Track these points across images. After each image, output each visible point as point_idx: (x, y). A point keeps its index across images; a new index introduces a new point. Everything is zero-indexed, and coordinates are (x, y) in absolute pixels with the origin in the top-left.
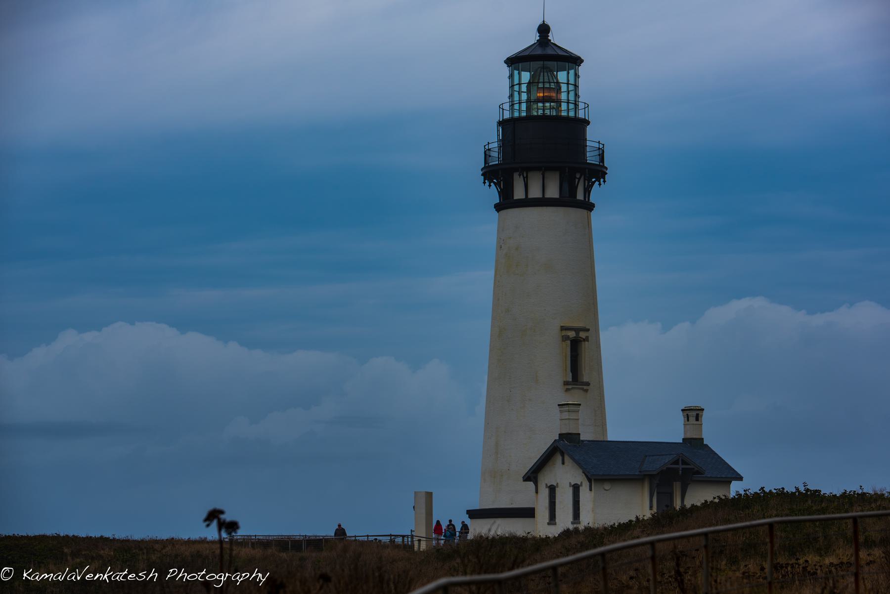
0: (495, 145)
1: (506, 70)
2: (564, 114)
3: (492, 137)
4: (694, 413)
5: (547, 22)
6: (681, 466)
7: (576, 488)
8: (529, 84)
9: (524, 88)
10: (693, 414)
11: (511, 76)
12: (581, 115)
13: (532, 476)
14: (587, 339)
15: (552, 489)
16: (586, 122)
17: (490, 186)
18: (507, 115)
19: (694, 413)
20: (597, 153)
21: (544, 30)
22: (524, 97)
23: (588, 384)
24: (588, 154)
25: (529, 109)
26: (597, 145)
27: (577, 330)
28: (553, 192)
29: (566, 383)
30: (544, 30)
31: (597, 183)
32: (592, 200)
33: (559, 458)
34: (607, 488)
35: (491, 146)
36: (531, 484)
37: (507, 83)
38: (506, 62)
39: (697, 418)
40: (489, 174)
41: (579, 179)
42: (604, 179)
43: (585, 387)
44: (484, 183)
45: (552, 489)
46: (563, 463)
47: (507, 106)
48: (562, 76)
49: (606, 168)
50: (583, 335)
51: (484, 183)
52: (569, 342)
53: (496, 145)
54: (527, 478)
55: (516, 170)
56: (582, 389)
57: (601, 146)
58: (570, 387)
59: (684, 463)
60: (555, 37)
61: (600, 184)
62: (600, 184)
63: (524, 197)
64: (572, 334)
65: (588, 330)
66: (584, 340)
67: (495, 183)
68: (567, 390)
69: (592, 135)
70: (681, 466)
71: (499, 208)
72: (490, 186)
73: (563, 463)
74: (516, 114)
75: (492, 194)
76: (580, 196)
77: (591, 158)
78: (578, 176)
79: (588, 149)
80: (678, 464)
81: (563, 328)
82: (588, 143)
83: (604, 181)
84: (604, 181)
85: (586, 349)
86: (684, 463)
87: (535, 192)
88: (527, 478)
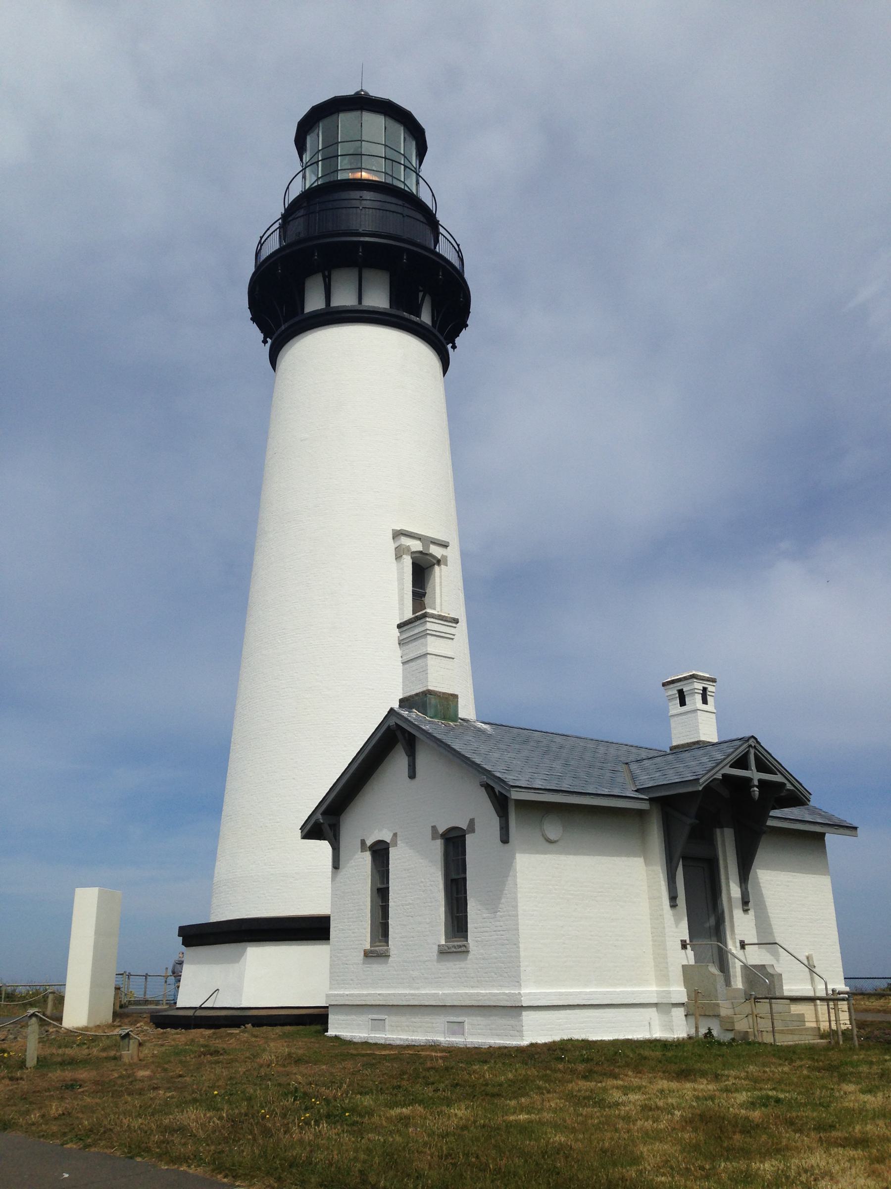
4: (699, 686)
6: (756, 776)
13: (325, 823)
15: (380, 853)
19: (699, 686)
33: (398, 762)
34: (552, 837)
36: (323, 847)
46: (412, 775)
50: (436, 551)
63: (323, 306)
65: (445, 545)
73: (412, 775)
81: (398, 534)
86: (762, 766)
88: (313, 830)
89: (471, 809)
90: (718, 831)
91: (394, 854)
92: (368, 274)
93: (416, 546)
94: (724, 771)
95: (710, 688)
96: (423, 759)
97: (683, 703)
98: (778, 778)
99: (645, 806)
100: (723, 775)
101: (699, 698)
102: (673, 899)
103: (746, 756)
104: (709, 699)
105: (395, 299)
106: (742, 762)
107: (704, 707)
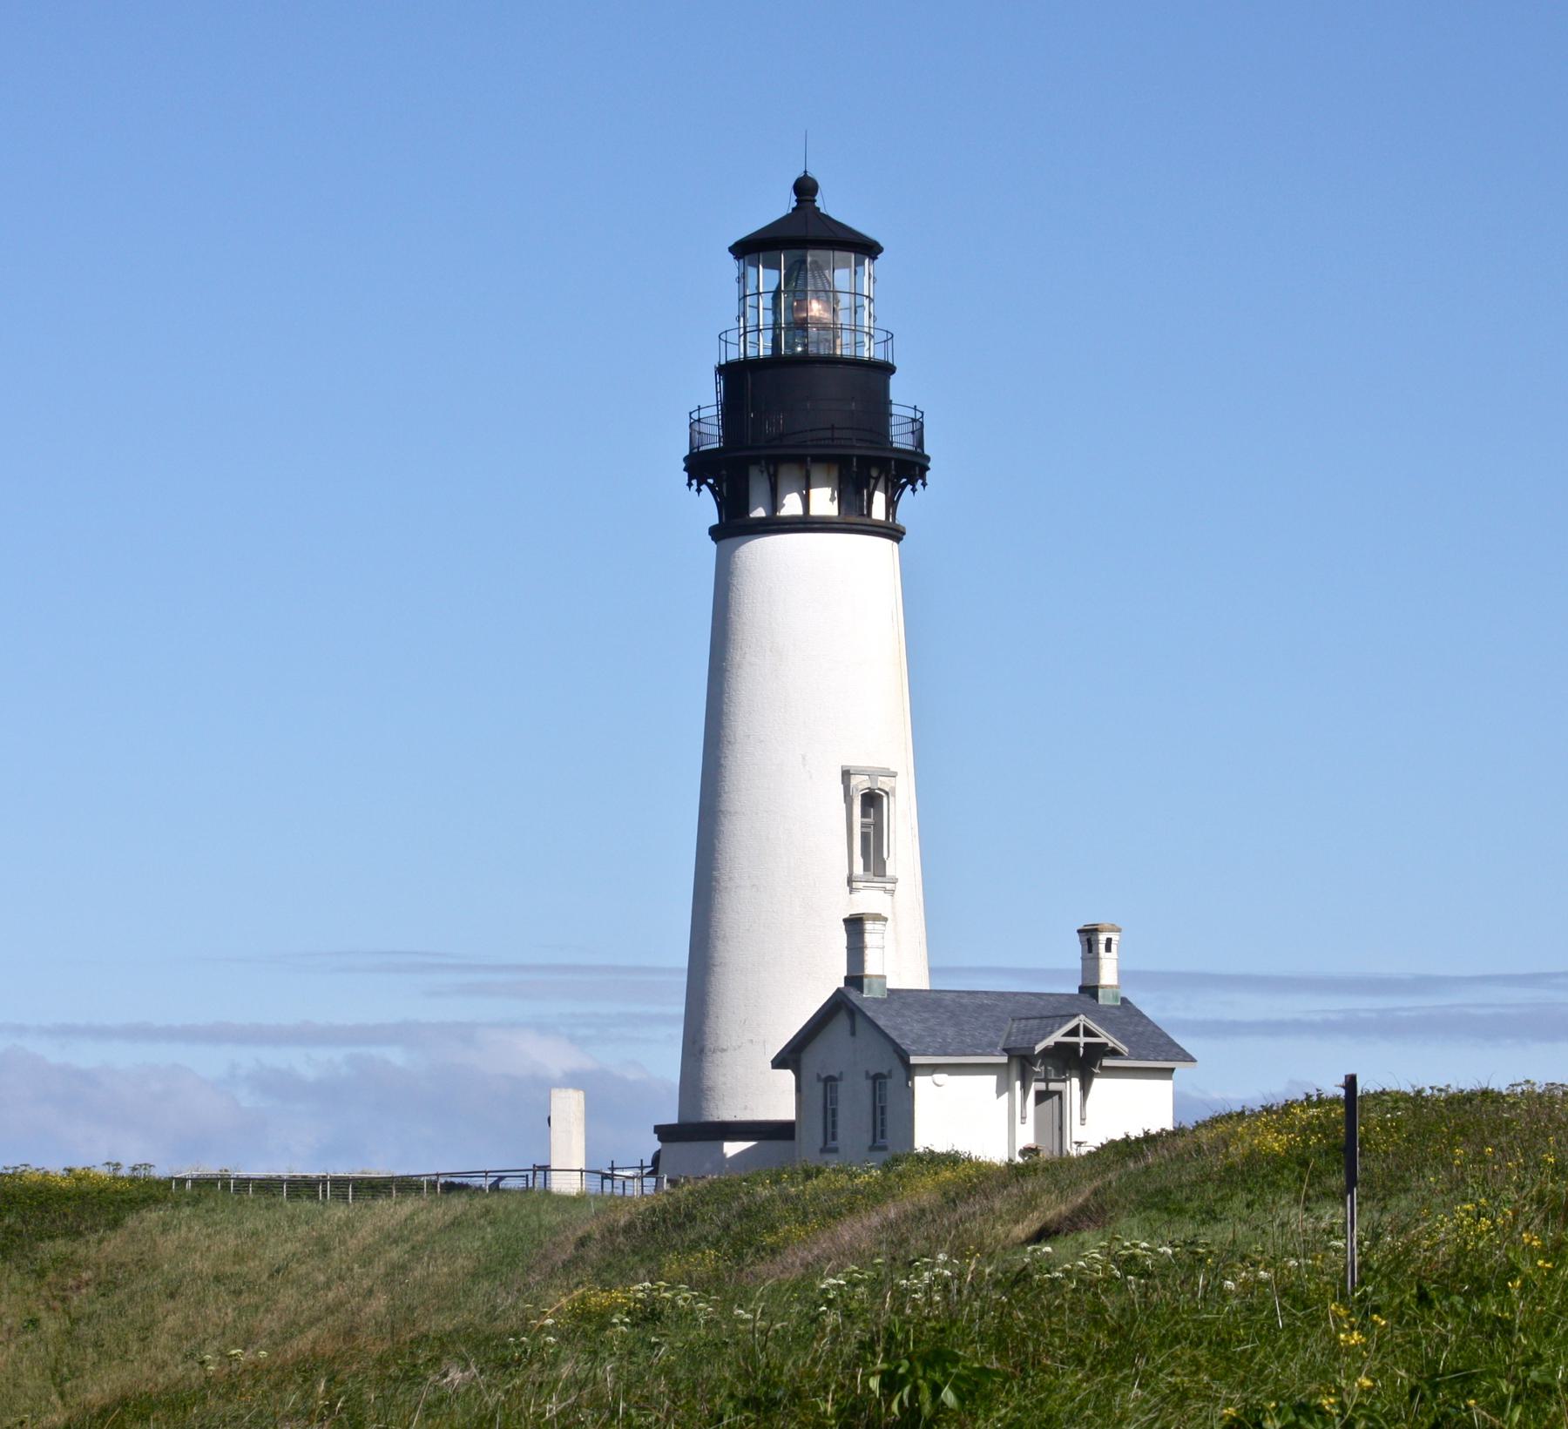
0: (712, 412)
1: (731, 265)
2: (847, 352)
3: (707, 395)
5: (812, 173)
7: (878, 1079)
8: (776, 295)
9: (765, 301)
11: (742, 279)
12: (880, 356)
16: (885, 369)
17: (699, 490)
18: (734, 354)
20: (910, 427)
21: (805, 189)
22: (766, 318)
24: (894, 430)
25: (776, 341)
26: (911, 414)
27: (872, 774)
28: (824, 502)
30: (805, 189)
31: (909, 487)
32: (902, 518)
35: (704, 413)
36: (788, 1076)
37: (734, 291)
38: (731, 250)
40: (699, 466)
41: (877, 480)
42: (923, 476)
43: (889, 886)
44: (690, 485)
45: (830, 1082)
46: (853, 1033)
47: (733, 337)
48: (842, 278)
49: (928, 459)
50: (883, 783)
51: (690, 485)
53: (713, 411)
54: (779, 1062)
55: (756, 461)
57: (919, 415)
58: (860, 885)
59: (1088, 1033)
60: (829, 203)
61: (914, 490)
62: (914, 490)
64: (860, 783)
65: (894, 775)
67: (709, 485)
69: (901, 392)
70: (1082, 1040)
71: (717, 533)
72: (699, 490)
73: (853, 1033)
74: (751, 353)
75: (705, 508)
76: (879, 510)
77: (901, 438)
78: (874, 473)
79: (894, 420)
82: (894, 409)
83: (924, 485)
84: (924, 485)
86: (1088, 1033)
87: (791, 505)
88: (779, 1062)
89: (889, 1063)
91: (842, 1087)
92: (817, 472)
95: (1115, 937)
96: (859, 1019)
97: (1090, 950)
99: (1004, 1060)
101: (1102, 947)
102: (1023, 1118)
104: (1114, 947)
106: (1074, 1032)
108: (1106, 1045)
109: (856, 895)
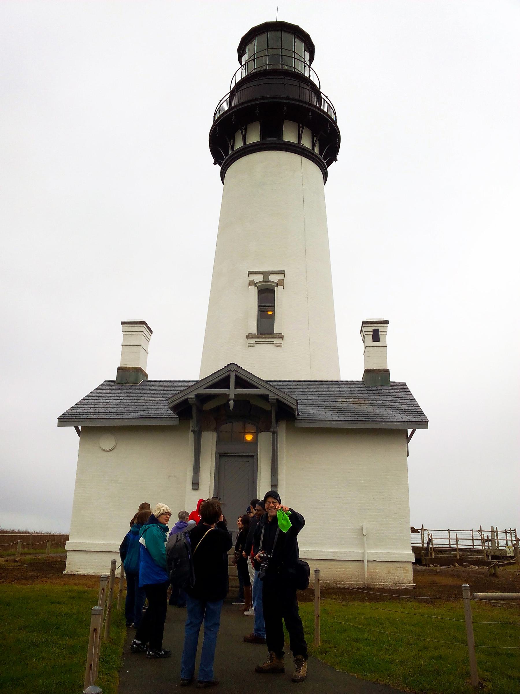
4: (370, 329)
10: (375, 331)
14: (281, 283)
23: (281, 337)
29: (249, 337)
39: (376, 336)
43: (276, 341)
50: (274, 278)
52: (254, 291)
56: (272, 343)
65: (283, 273)
66: (277, 285)
68: (250, 345)
70: (232, 392)
80: (228, 387)
85: (282, 298)
90: (259, 434)
93: (259, 278)
94: (197, 392)
98: (261, 391)
100: (197, 396)
103: (228, 378)
105: (264, 135)
107: (376, 344)
108: (268, 395)
109: (252, 349)
